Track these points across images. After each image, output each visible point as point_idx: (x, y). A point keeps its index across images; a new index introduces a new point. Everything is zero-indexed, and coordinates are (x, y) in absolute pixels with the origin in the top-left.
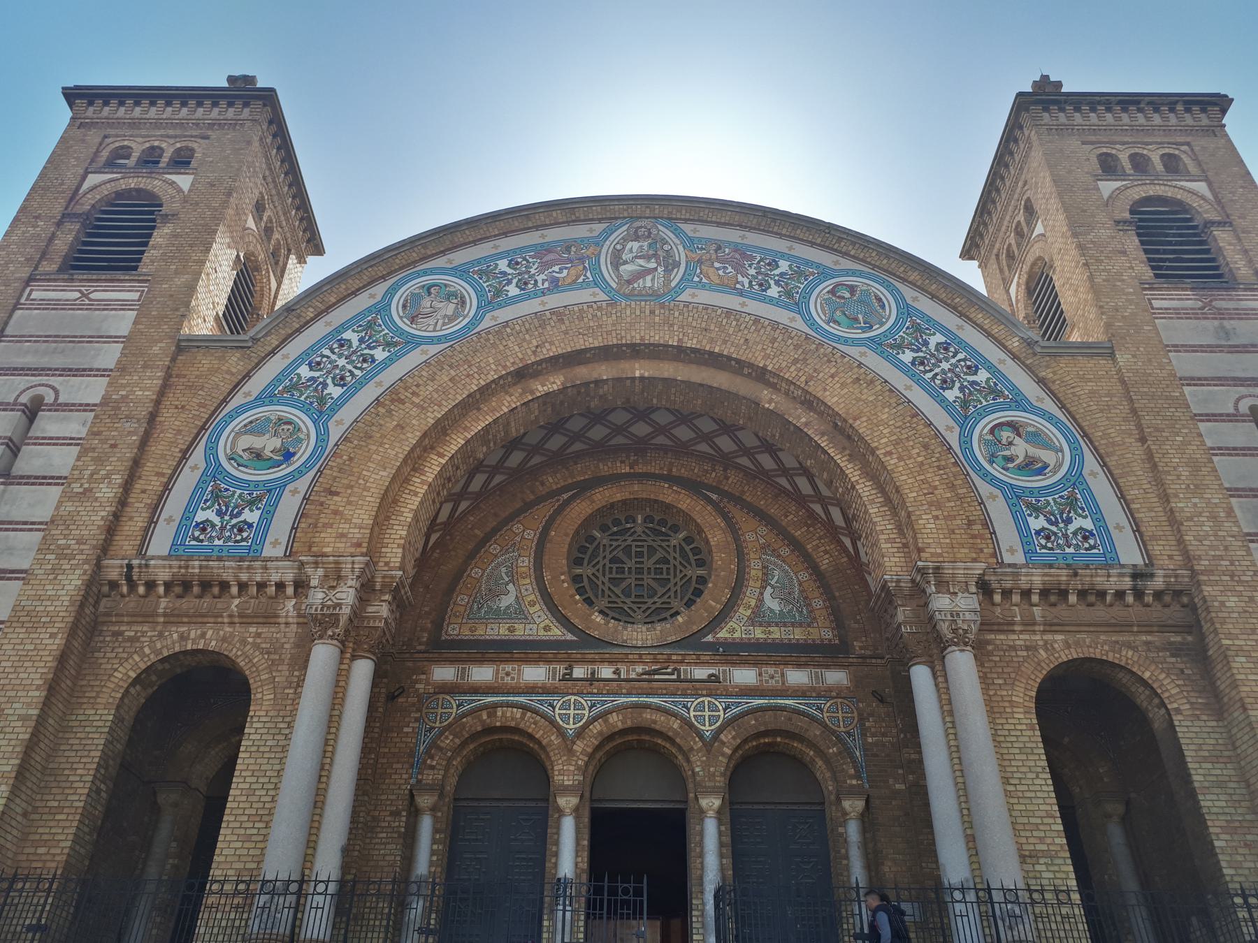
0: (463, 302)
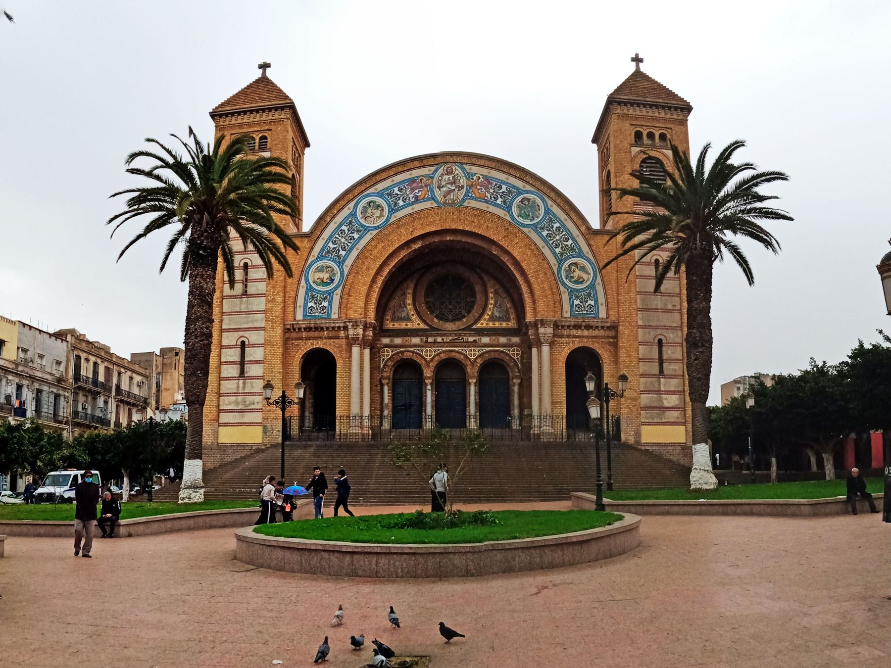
0: (383, 210)
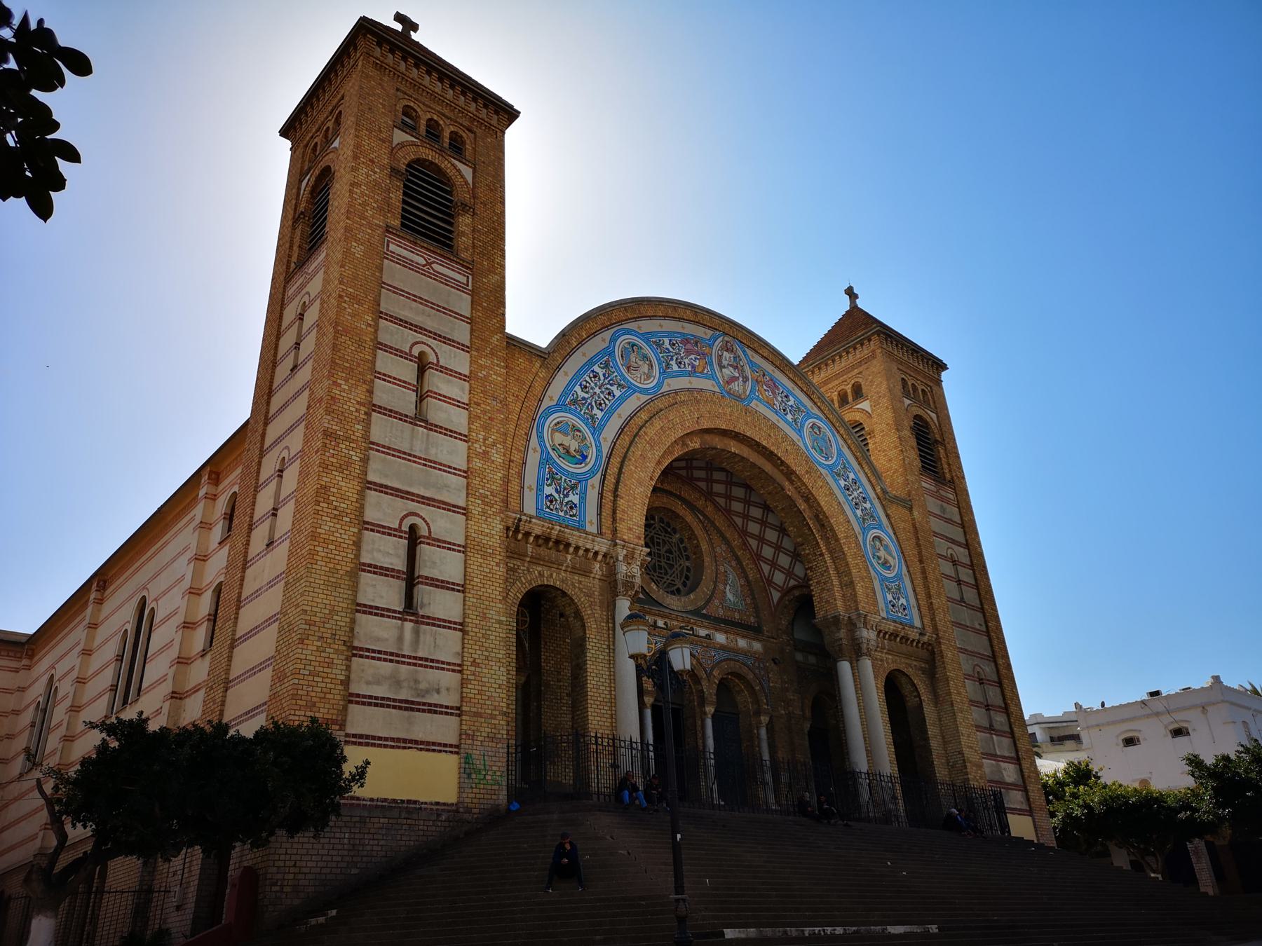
0: (652, 366)
